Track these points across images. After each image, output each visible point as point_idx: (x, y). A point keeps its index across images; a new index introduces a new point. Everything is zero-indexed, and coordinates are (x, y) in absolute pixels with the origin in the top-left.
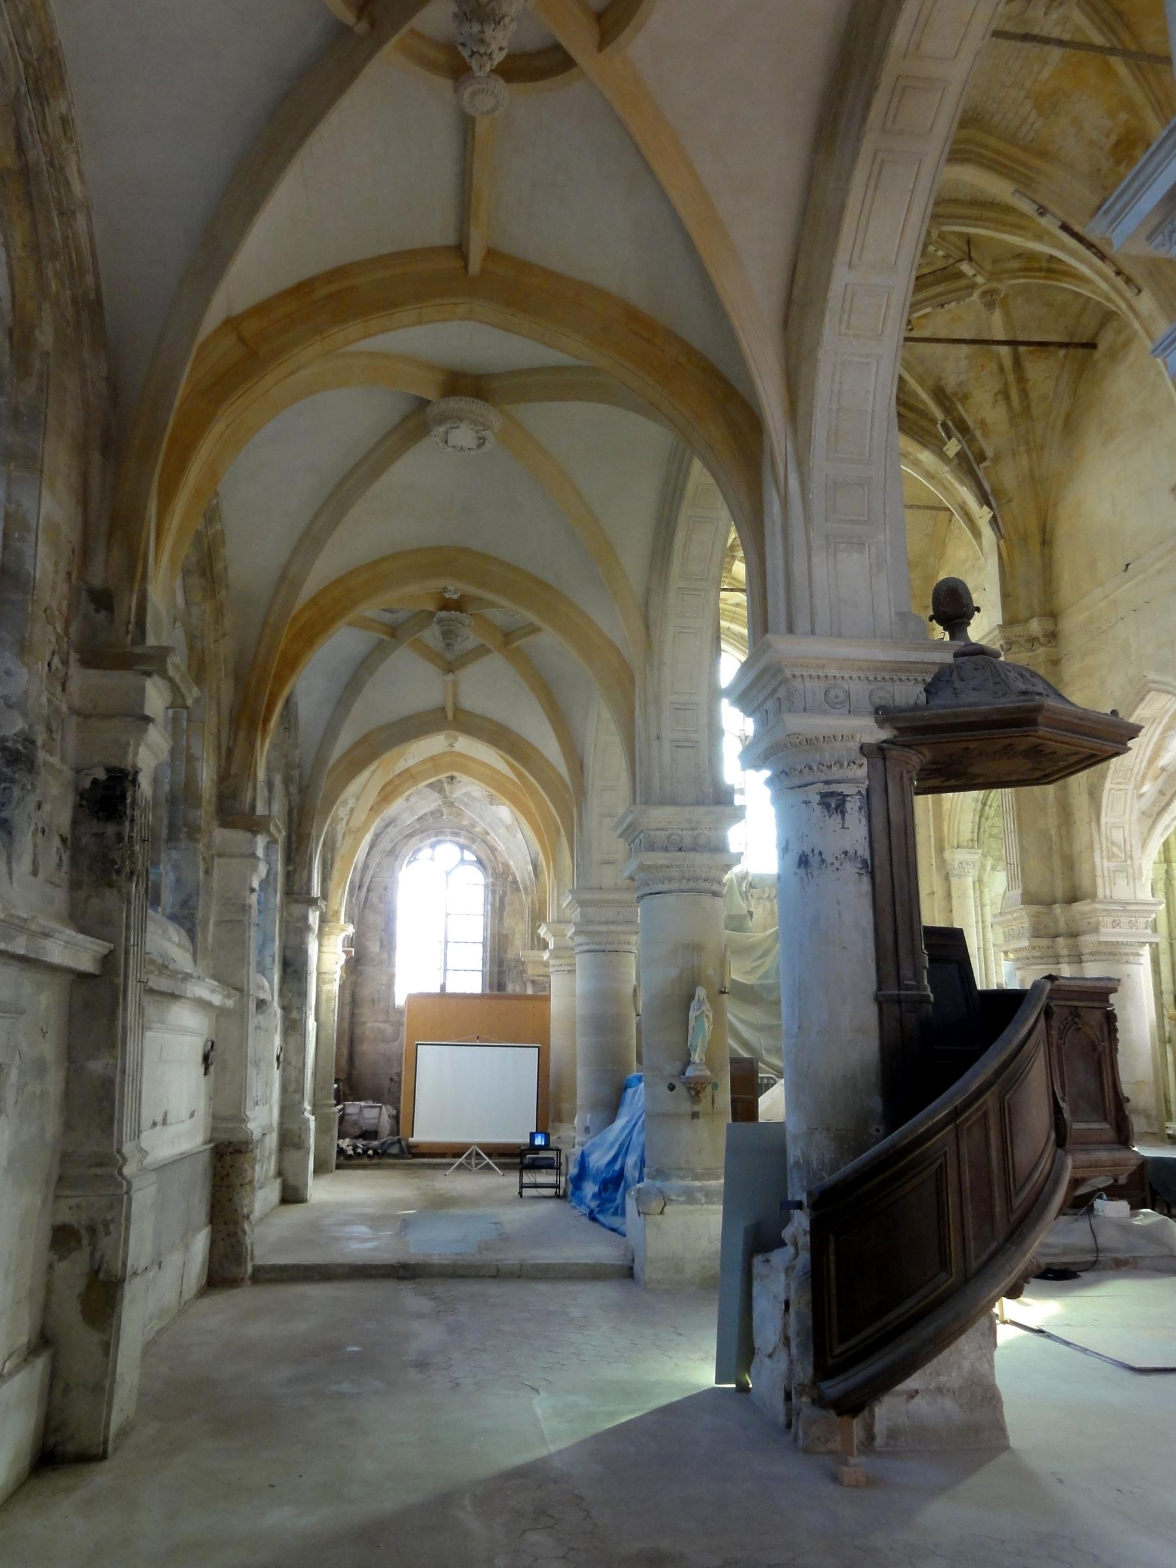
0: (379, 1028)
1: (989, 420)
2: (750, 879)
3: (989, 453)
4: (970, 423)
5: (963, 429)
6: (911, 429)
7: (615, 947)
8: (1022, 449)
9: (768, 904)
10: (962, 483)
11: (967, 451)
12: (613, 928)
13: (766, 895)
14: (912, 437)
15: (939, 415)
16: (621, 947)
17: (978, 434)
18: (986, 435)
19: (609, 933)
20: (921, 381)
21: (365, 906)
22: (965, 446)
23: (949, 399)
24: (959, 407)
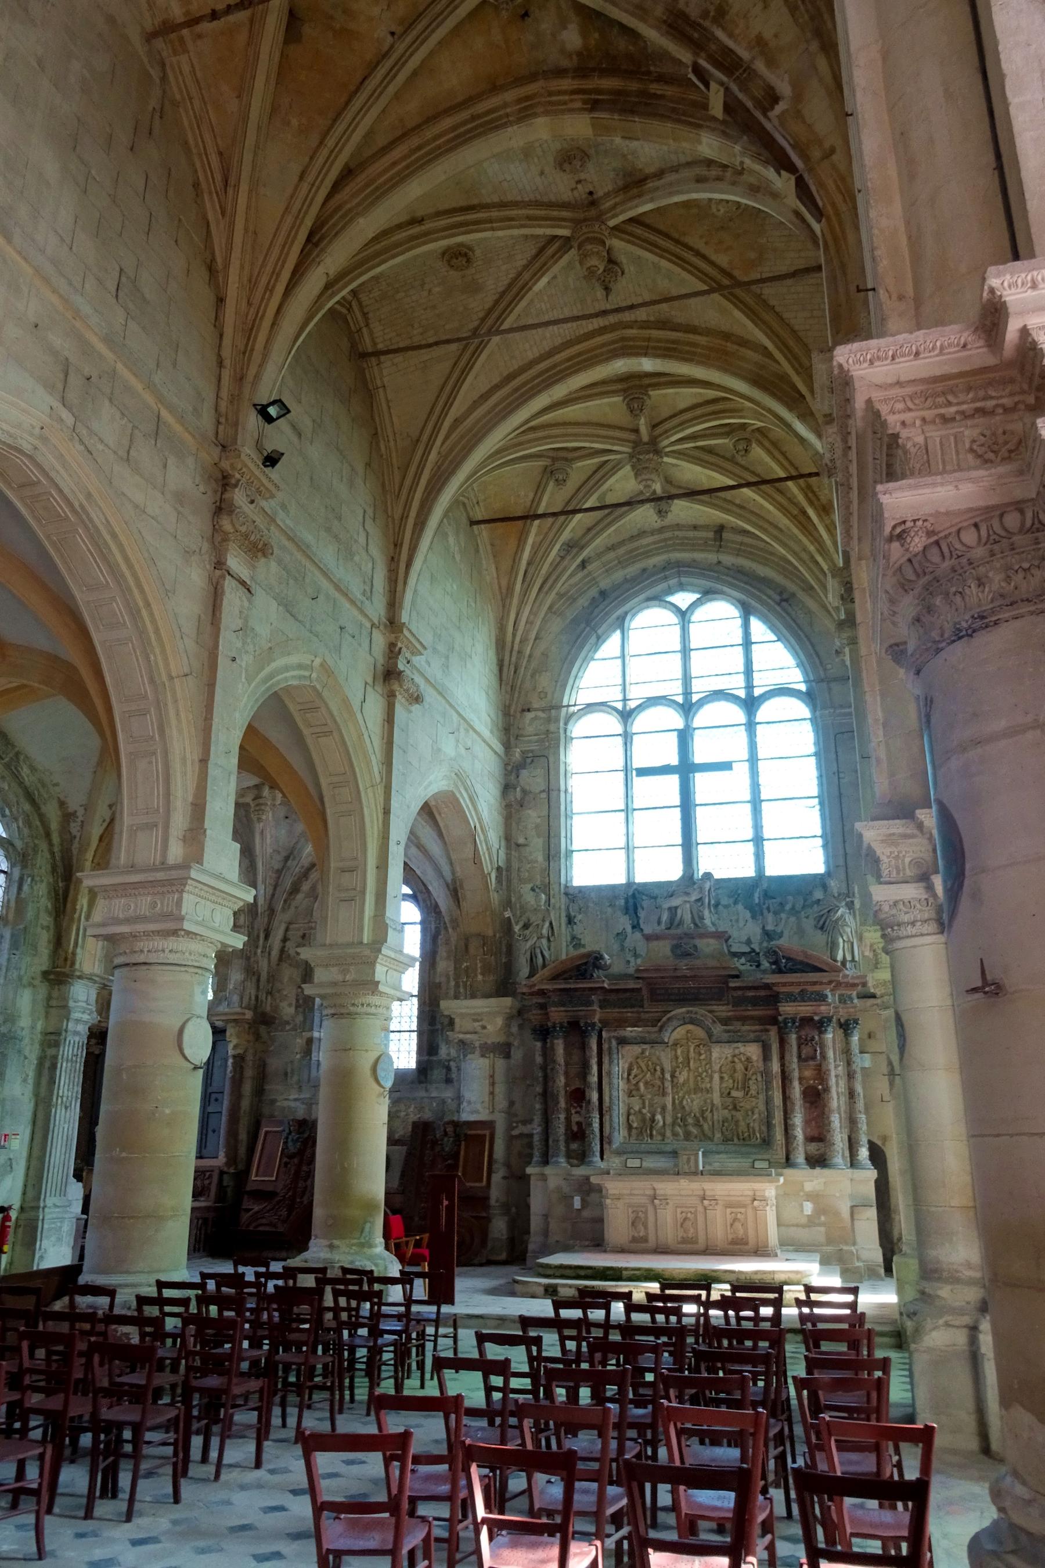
0: (289, 1107)
1: (768, 35)
2: (765, 886)
3: (784, 88)
4: (744, 54)
5: (729, 63)
6: (674, 110)
7: (142, 958)
8: (814, 46)
9: (793, 919)
10: (766, 162)
11: (741, 96)
12: (140, 927)
13: (788, 907)
14: (679, 121)
15: (685, 56)
16: (152, 958)
17: (760, 66)
18: (771, 63)
19: (134, 936)
20: (641, 11)
21: (280, 959)
22: (734, 88)
23: (695, 25)
24: (720, 34)
